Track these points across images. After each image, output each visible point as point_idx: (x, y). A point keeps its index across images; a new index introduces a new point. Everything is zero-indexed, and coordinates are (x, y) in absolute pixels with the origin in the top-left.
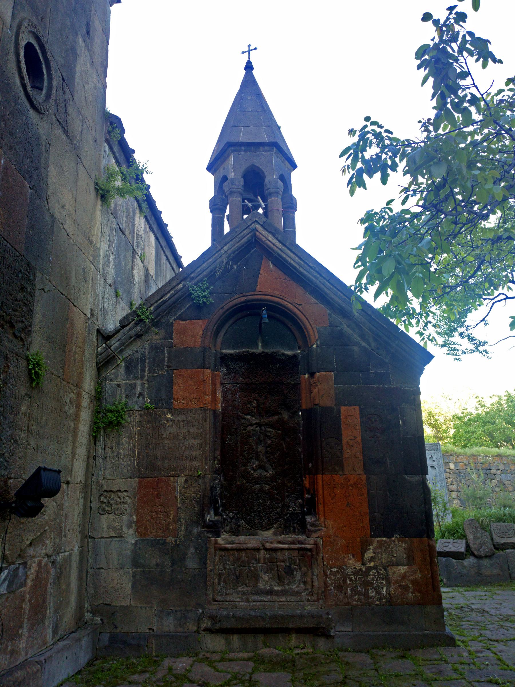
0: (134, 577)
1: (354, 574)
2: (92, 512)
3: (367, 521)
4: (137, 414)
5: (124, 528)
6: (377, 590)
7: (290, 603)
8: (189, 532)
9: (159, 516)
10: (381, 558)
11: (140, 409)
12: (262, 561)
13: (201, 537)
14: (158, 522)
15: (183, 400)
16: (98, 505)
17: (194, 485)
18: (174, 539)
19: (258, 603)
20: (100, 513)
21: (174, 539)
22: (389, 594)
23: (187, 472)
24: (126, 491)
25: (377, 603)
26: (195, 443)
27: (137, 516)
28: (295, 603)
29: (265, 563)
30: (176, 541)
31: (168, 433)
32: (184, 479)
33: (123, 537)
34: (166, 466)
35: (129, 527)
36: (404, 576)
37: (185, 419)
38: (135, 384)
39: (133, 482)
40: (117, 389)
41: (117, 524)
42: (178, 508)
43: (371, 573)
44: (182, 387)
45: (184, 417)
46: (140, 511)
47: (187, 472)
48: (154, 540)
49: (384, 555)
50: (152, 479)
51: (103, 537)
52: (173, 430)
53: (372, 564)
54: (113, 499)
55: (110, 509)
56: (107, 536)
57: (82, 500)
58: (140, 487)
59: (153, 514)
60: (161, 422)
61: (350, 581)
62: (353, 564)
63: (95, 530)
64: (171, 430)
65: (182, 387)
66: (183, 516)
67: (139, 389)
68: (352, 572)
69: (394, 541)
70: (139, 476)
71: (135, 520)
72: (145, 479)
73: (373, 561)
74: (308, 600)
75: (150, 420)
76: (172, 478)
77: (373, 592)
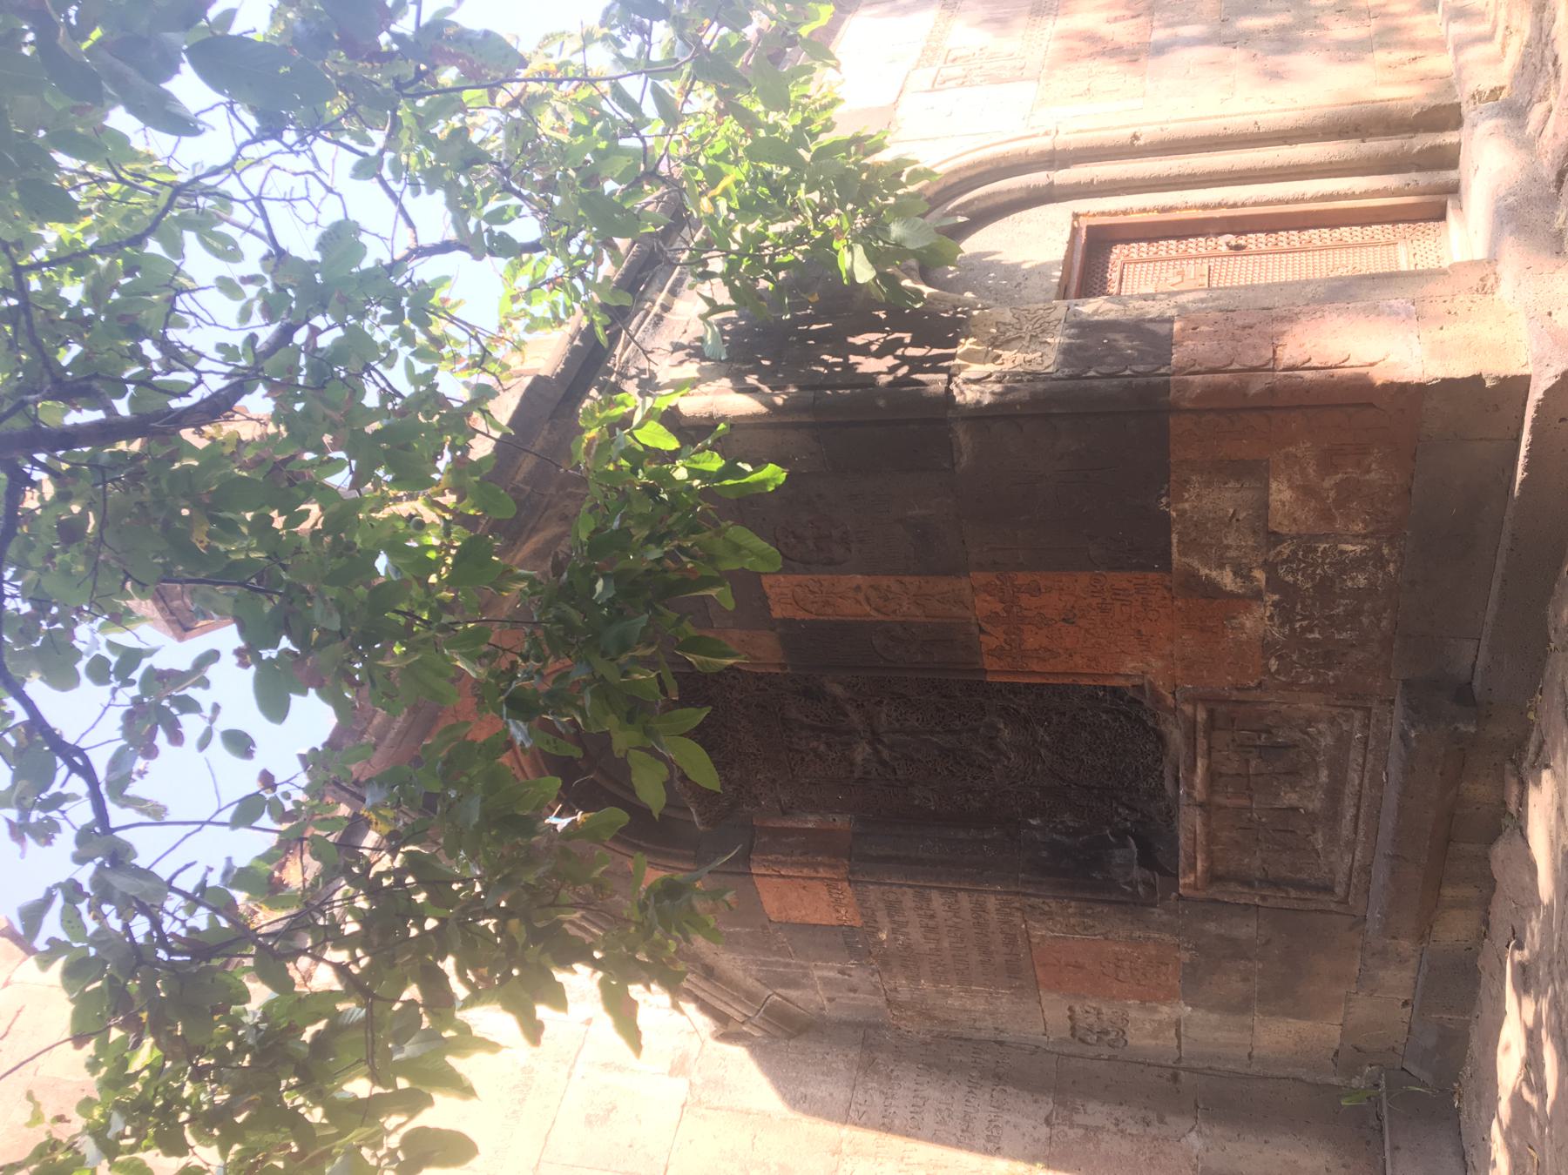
0: (1272, 1014)
1: (1291, 622)
3: (1120, 579)
5: (1157, 1017)
6: (1346, 566)
7: (1368, 766)
10: (1239, 547)
12: (1244, 802)
19: (1361, 826)
22: (1365, 537)
25: (1391, 567)
28: (1370, 757)
29: (1251, 798)
30: (1187, 949)
36: (1307, 492)
43: (1290, 579)
49: (1229, 541)
51: (1179, 1047)
53: (1259, 575)
57: (1092, 1106)
61: (1312, 631)
62: (1255, 622)
68: (1282, 625)
69: (1182, 514)
73: (1250, 570)
74: (1366, 726)
77: (1352, 579)
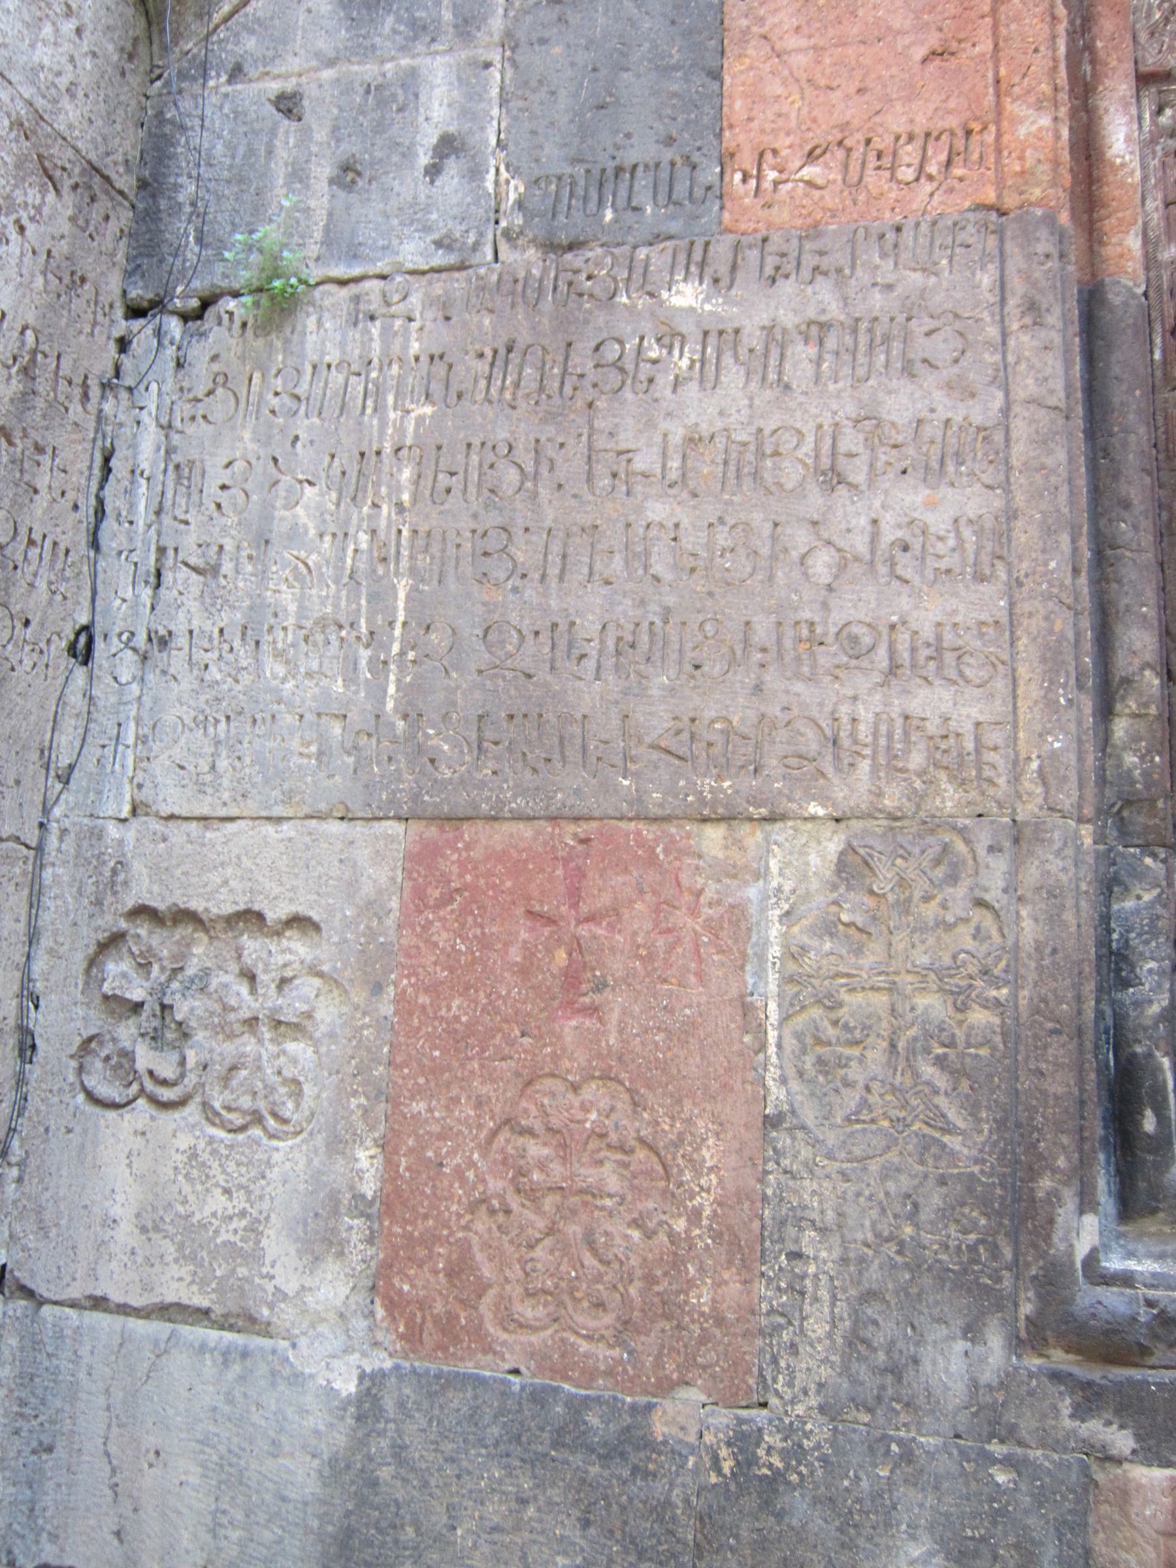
2: (34, 1072)
4: (415, 300)
5: (277, 1246)
8: (882, 1382)
9: (590, 1175)
11: (440, 259)
13: (1009, 1434)
14: (574, 1230)
15: (811, 156)
16: (92, 1020)
17: (930, 911)
18: (723, 1418)
20: (91, 1097)
21: (723, 1418)
23: (857, 786)
24: (299, 922)
26: (938, 522)
27: (388, 1147)
30: (744, 1441)
31: (678, 434)
32: (833, 845)
33: (266, 1330)
34: (657, 720)
35: (321, 1243)
37: (835, 311)
38: (411, 80)
39: (362, 855)
40: (273, 132)
41: (218, 1202)
42: (772, 1122)
44: (800, 61)
45: (825, 298)
46: (419, 1106)
47: (857, 786)
48: (539, 1397)
50: (525, 831)
51: (99, 1303)
52: (727, 405)
54: (200, 985)
55: (167, 1071)
56: (136, 1301)
58: (419, 894)
59: (536, 1150)
60: (612, 352)
63: (43, 1229)
64: (698, 410)
65: (800, 61)
66: (816, 1194)
67: (437, 112)
70: (416, 797)
71: (369, 1188)
72: (468, 831)
75: (524, 338)
76: (713, 837)
